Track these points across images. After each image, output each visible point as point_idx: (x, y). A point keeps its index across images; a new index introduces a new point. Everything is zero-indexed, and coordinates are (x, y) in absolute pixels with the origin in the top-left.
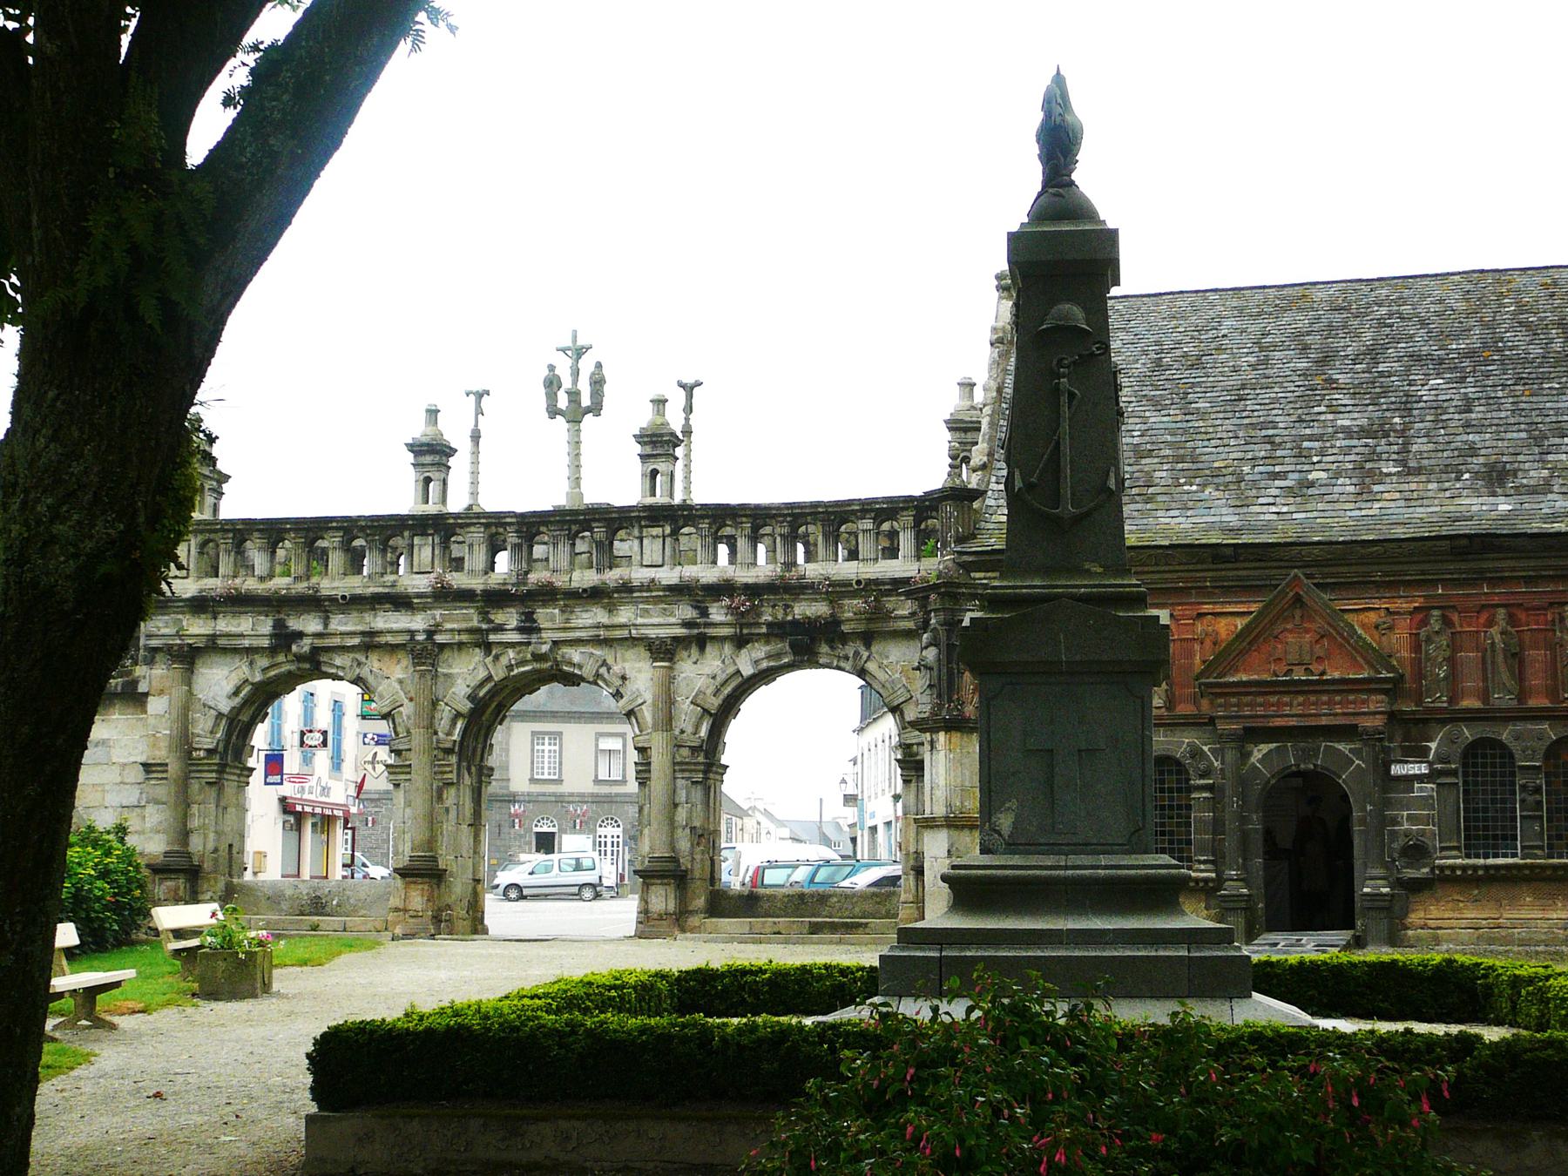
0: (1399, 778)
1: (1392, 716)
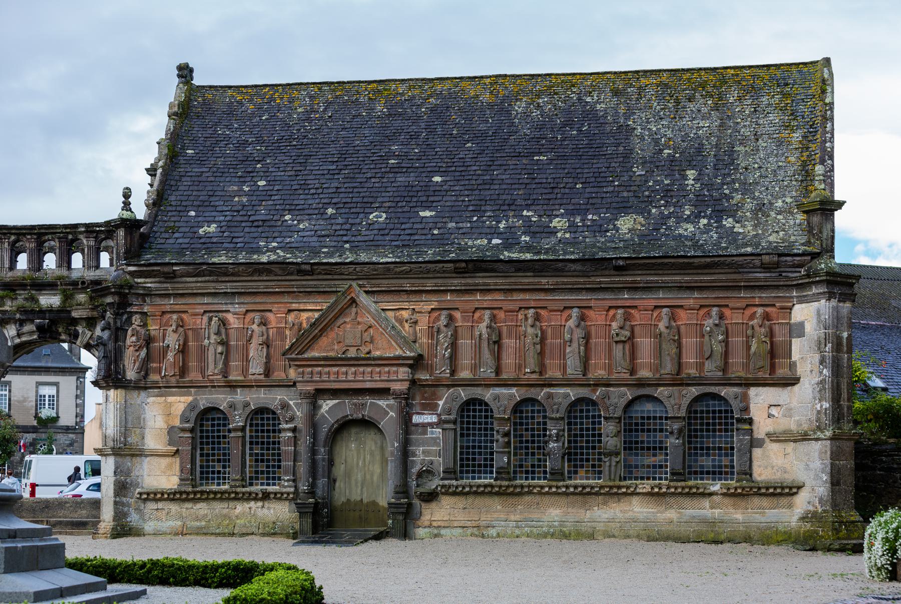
0: (417, 425)
1: (413, 382)
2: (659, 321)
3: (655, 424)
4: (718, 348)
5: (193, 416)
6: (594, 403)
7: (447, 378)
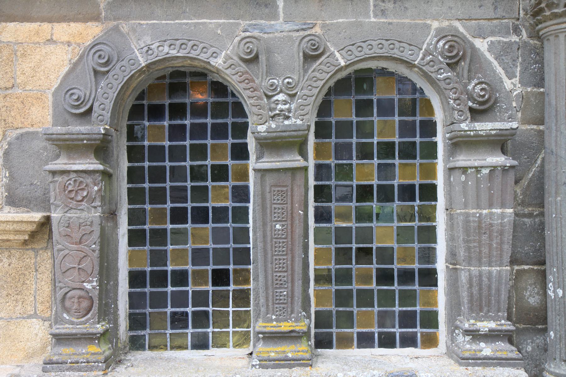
5: (106, 96)
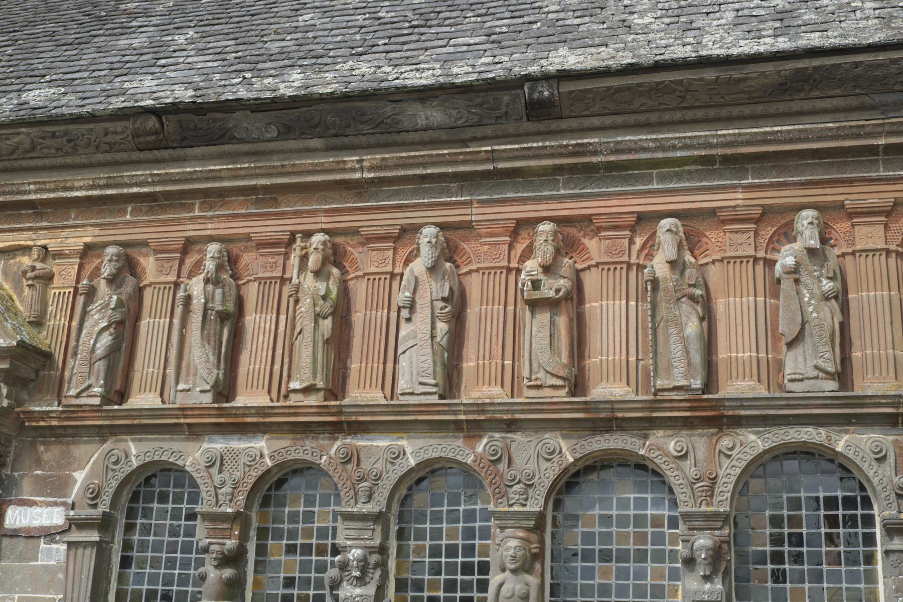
0: (15, 534)
2: (650, 256)
3: (641, 538)
4: (825, 316)
6: (470, 478)
7: (94, 409)
